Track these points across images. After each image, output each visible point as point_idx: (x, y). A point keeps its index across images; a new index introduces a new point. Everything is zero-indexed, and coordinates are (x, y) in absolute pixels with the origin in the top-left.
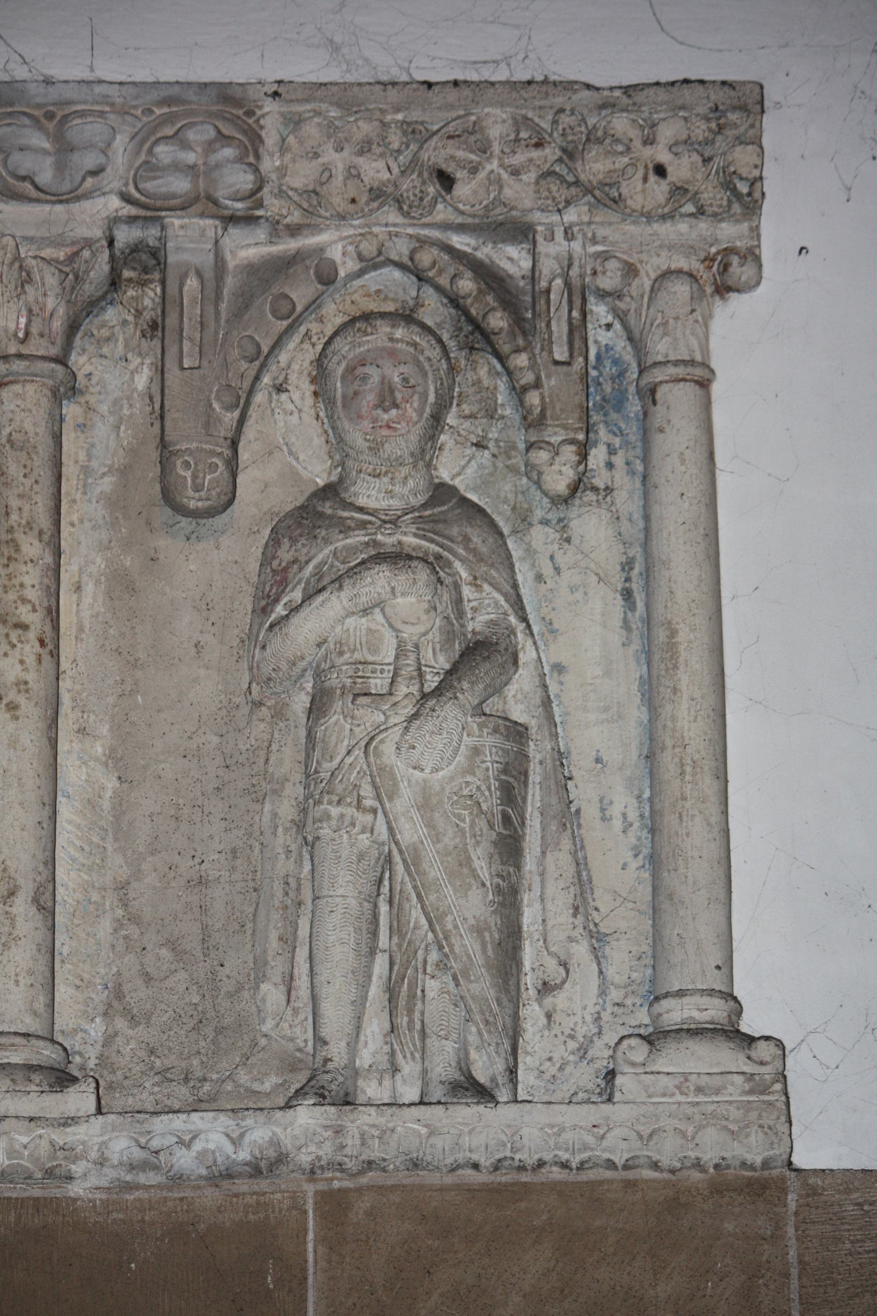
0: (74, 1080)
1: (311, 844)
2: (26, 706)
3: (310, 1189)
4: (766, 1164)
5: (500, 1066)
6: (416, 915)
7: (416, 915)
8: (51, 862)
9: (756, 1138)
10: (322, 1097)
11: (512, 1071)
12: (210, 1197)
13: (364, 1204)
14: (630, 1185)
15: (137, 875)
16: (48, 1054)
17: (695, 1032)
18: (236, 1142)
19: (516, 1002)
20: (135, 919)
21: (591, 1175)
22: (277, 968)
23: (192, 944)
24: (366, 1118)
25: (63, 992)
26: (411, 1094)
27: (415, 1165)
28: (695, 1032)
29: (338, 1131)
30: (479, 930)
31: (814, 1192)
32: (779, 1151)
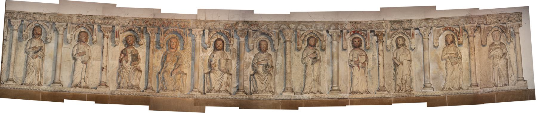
0: (478, 86)
1: (493, 68)
2: (474, 60)
3: (495, 93)
4: (526, 89)
5: (507, 83)
6: (501, 73)
7: (501, 73)
8: (476, 71)
9: (525, 87)
10: (495, 86)
11: (508, 84)
12: (488, 94)
13: (499, 93)
14: (517, 91)
15: (482, 71)
16: (477, 84)
17: (520, 80)
18: (490, 90)
19: (508, 78)
20: (482, 74)
21: (514, 90)
22: (492, 77)
23: (486, 75)
24: (498, 88)
25: (477, 79)
26: (501, 86)
27: (502, 90)
28: (520, 80)
29: (497, 89)
30: (505, 74)
31: (529, 91)
32: (527, 88)
